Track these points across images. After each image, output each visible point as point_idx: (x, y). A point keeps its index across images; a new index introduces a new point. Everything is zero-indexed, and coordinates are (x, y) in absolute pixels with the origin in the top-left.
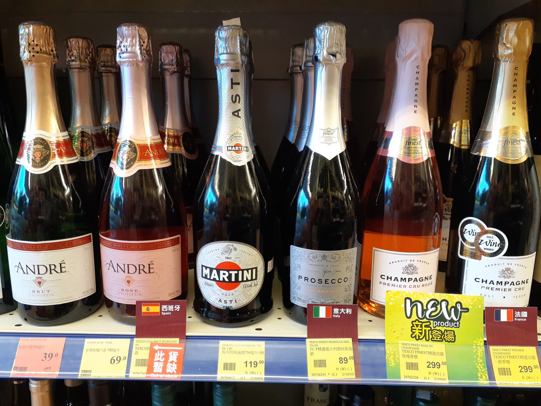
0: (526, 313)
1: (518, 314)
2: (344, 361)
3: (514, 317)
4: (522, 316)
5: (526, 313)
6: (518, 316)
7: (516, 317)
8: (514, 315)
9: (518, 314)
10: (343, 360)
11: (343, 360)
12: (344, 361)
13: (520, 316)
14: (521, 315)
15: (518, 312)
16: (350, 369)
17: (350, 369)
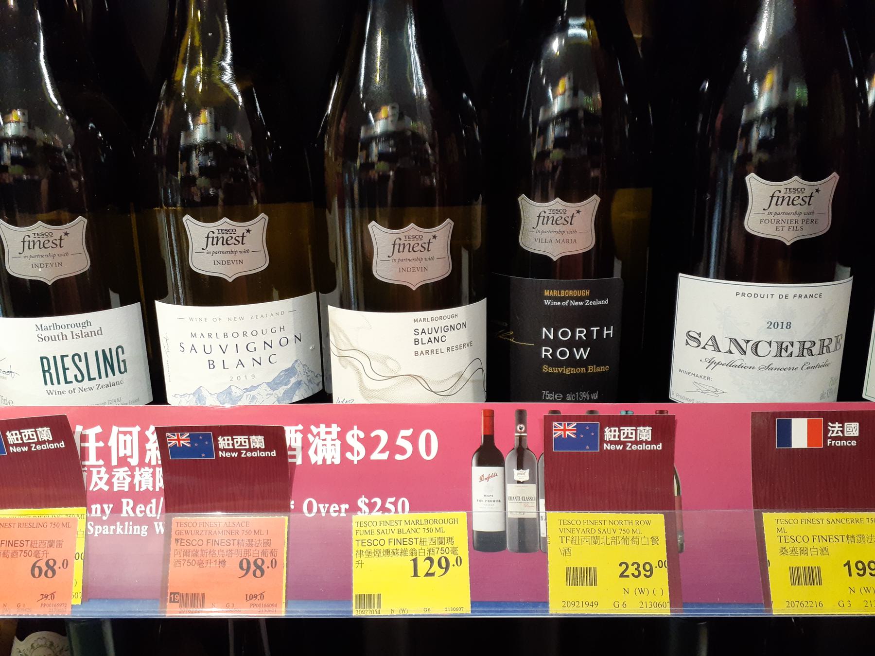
0: (856, 425)
1: (836, 430)
2: (643, 572)
3: (826, 438)
4: (846, 435)
5: (856, 425)
6: (834, 435)
7: (831, 438)
8: (826, 431)
9: (835, 429)
10: (641, 569)
11: (641, 569)
12: (643, 572)
13: (840, 434)
14: (842, 432)
15: (837, 425)
16: (658, 592)
17: (658, 592)
